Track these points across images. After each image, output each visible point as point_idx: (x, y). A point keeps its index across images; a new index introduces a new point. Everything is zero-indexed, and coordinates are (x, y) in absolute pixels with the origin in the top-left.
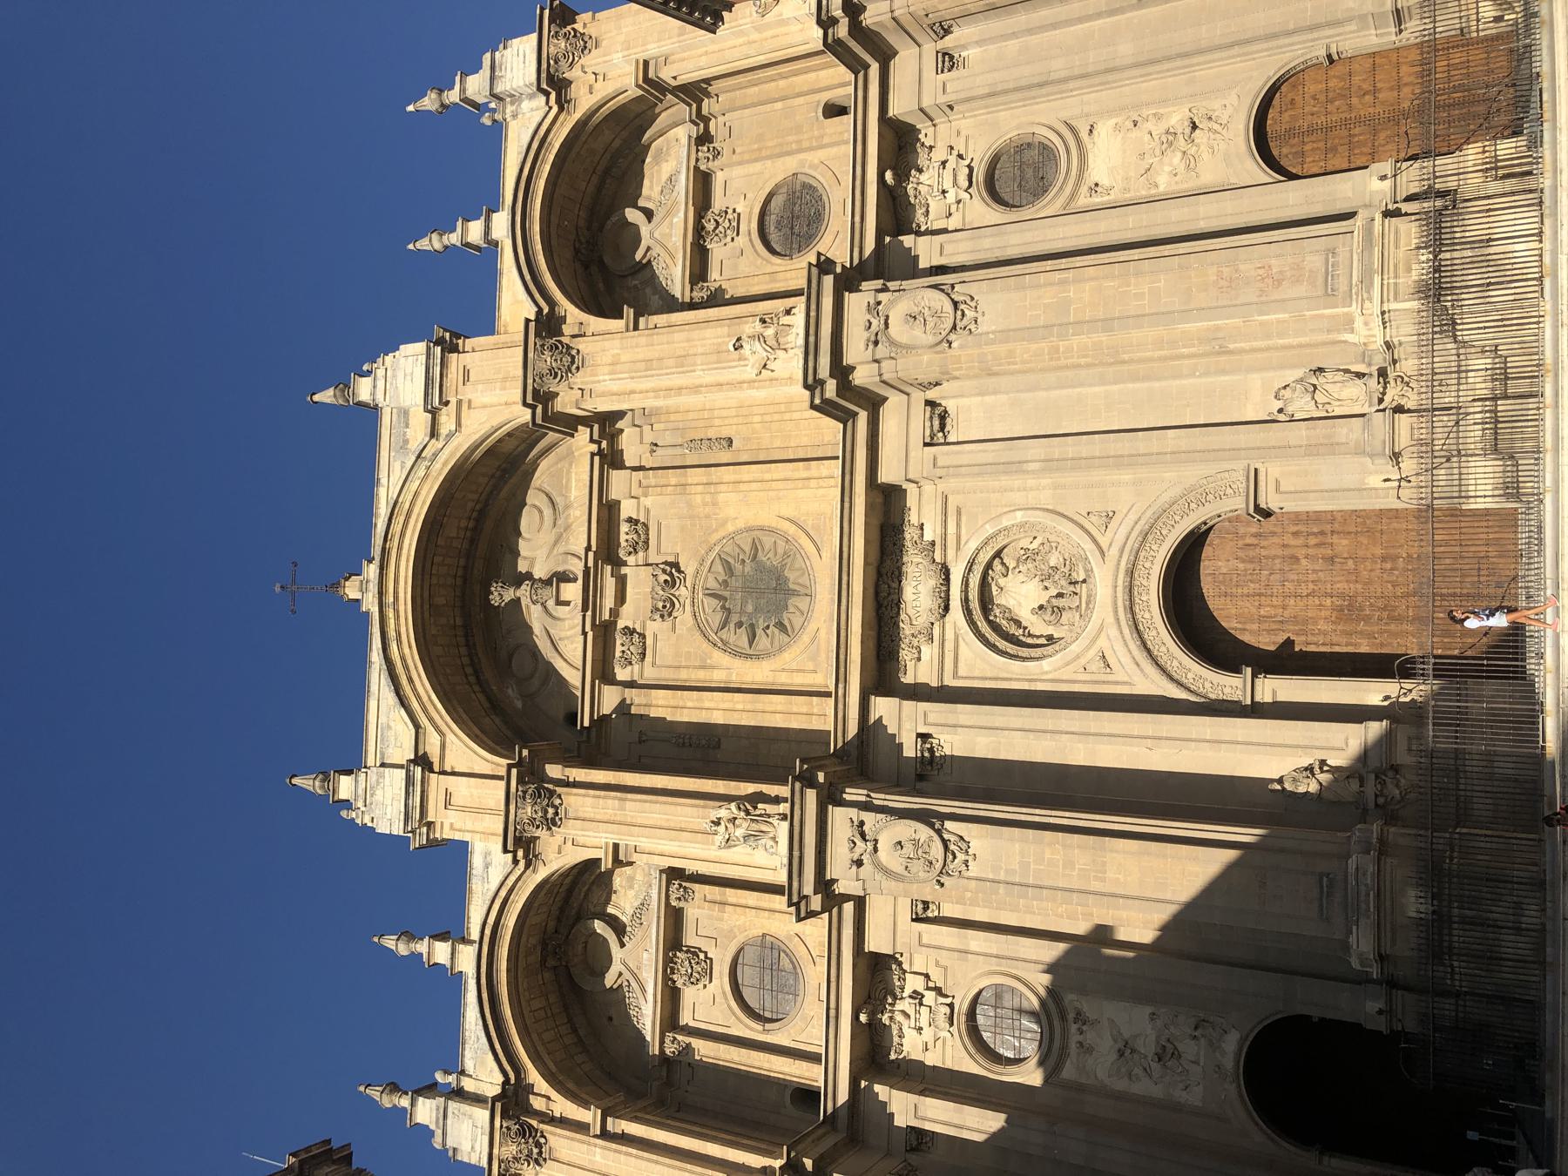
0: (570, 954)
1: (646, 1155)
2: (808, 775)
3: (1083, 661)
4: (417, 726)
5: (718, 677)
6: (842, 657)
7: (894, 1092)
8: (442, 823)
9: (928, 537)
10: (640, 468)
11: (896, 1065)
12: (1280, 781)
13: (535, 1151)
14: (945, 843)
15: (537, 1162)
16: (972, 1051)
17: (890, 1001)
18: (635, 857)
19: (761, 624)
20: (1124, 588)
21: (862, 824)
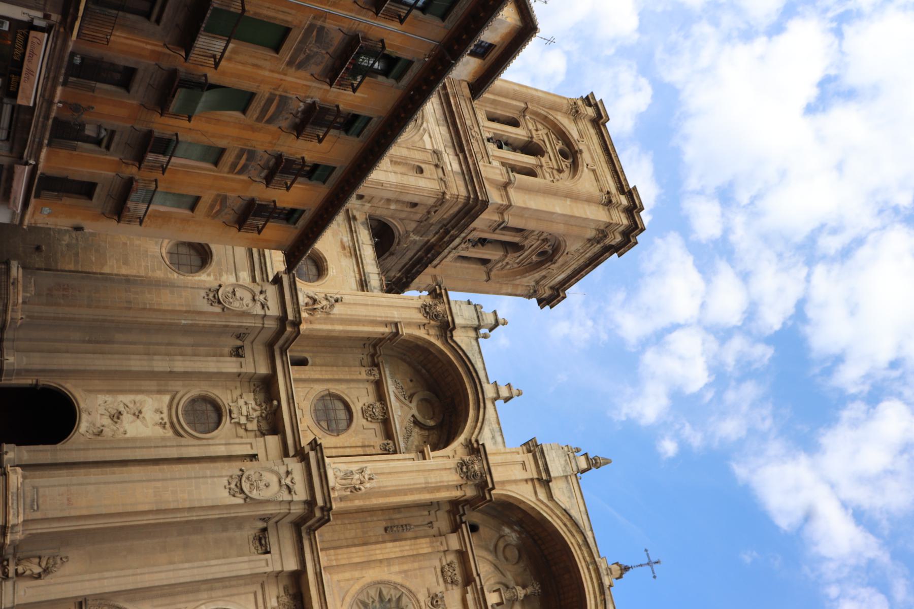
1: (372, 318)
2: (325, 513)
6: (321, 587)
7: (253, 371)
8: (524, 453)
13: (428, 310)
14: (242, 491)
15: (426, 306)
17: (264, 415)
18: (413, 455)
19: (377, 605)
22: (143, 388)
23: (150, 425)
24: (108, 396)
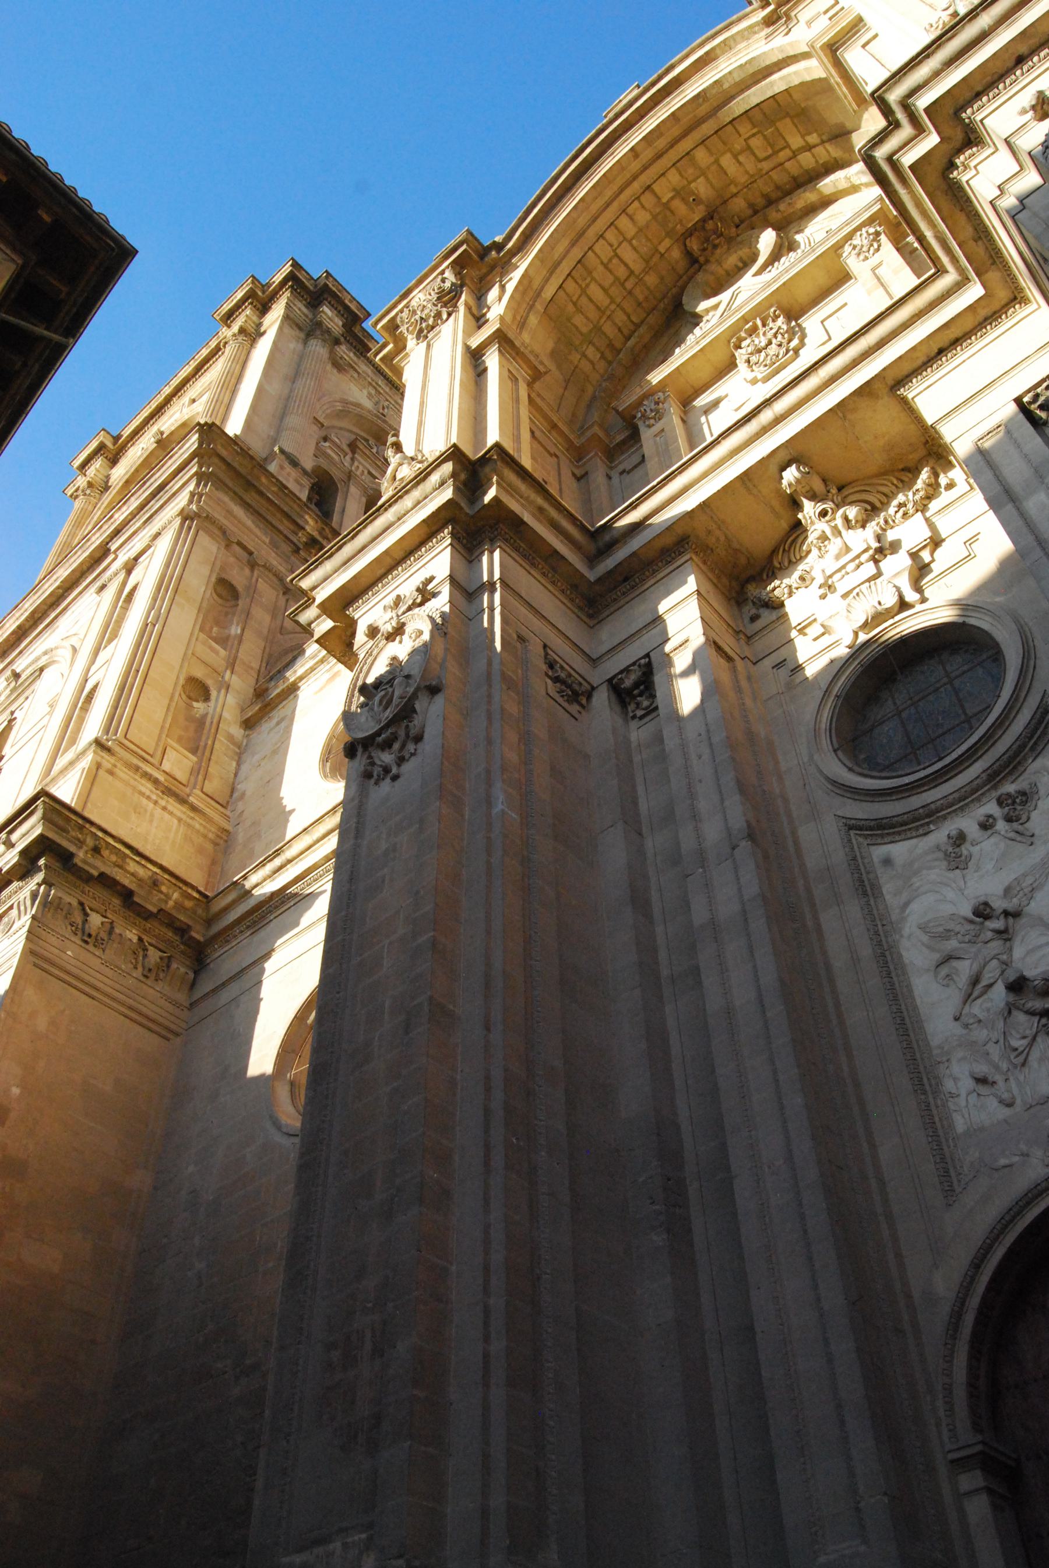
0: (718, 251)
11: (754, 611)
13: (431, 321)
17: (852, 512)
22: (866, 950)
23: (1038, 853)
24: (949, 1085)
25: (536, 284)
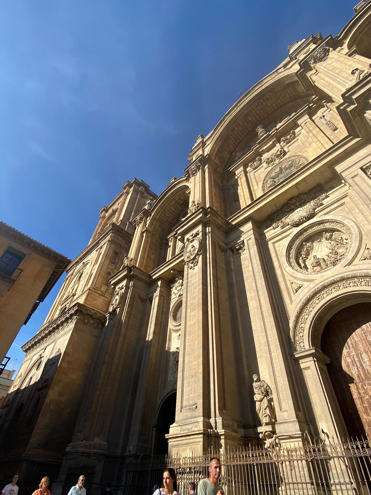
3: (295, 281)
4: (211, 137)
5: (256, 187)
9: (324, 202)
10: (313, 121)
12: (259, 380)
14: (194, 258)
16: (175, 305)
20: (334, 280)
21: (198, 234)
25: (155, 216)
